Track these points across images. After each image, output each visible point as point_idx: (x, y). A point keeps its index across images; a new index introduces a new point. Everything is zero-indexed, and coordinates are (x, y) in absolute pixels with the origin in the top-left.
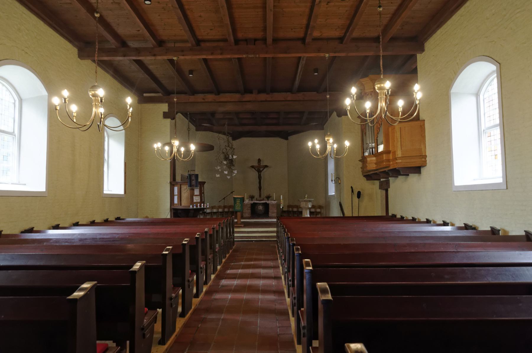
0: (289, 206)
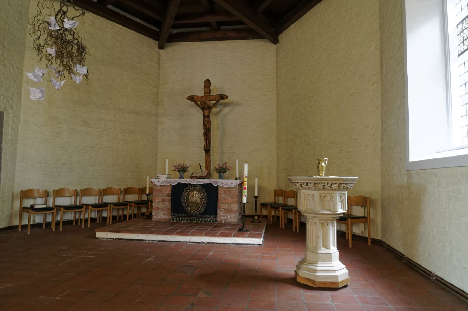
0: (278, 193)
